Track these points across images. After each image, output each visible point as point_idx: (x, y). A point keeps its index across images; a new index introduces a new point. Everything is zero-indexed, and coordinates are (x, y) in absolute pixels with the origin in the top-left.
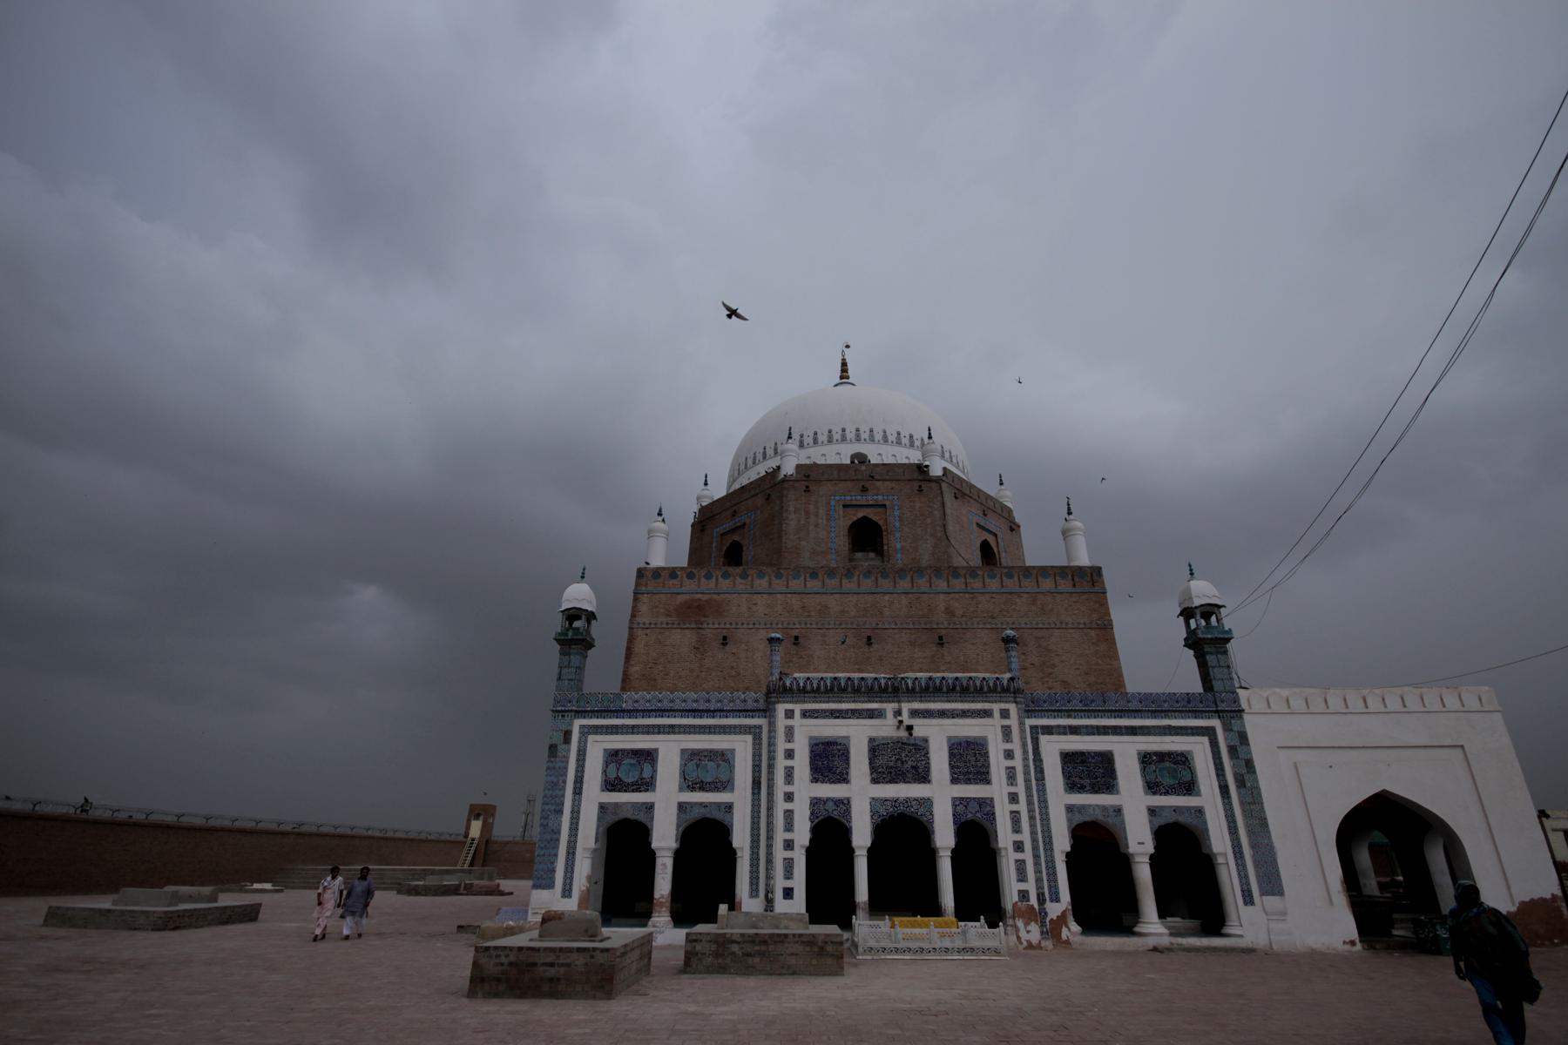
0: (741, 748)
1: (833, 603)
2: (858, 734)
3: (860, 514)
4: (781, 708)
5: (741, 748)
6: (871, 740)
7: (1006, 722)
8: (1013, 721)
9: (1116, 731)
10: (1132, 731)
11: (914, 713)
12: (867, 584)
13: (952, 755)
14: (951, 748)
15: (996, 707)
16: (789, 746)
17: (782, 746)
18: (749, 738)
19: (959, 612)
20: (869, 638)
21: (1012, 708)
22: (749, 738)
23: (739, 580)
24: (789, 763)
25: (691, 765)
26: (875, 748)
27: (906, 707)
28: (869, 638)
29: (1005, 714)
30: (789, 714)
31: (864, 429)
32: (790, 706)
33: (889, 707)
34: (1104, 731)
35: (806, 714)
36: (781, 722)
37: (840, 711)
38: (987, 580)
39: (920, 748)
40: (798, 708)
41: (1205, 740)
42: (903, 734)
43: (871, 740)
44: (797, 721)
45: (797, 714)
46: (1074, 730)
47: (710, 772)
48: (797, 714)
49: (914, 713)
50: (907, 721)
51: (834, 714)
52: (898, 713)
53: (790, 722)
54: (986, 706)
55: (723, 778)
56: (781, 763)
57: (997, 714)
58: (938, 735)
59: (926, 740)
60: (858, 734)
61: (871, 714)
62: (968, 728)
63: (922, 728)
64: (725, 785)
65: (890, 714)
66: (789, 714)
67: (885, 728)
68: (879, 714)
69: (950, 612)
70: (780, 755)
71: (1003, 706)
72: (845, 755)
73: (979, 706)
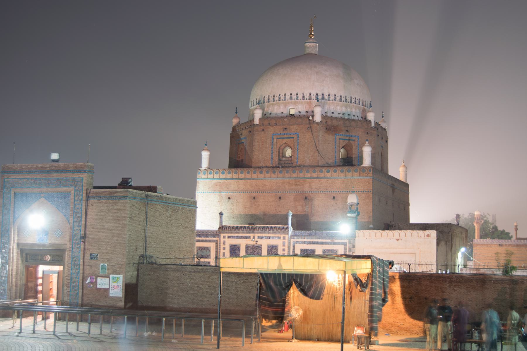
0: (212, 246)
1: (268, 183)
2: (243, 243)
3: (284, 142)
4: (222, 235)
5: (212, 246)
6: (246, 245)
7: (284, 240)
8: (286, 241)
9: (318, 243)
10: (322, 243)
11: (259, 237)
12: (281, 175)
13: (268, 250)
14: (268, 248)
15: (282, 236)
16: (224, 246)
17: (222, 246)
18: (215, 243)
19: (314, 187)
20: (280, 198)
21: (287, 236)
22: (215, 243)
23: (234, 175)
24: (224, 251)
25: (199, 251)
26: (247, 247)
27: (256, 235)
28: (280, 198)
29: (284, 238)
30: (224, 237)
31: (294, 93)
32: (224, 235)
33: (251, 235)
34: (314, 243)
35: (229, 237)
36: (222, 240)
37: (238, 236)
38: (326, 173)
39: (260, 247)
40: (227, 235)
41: (343, 247)
42: (255, 243)
43: (246, 245)
44: (226, 239)
45: (226, 237)
46: (304, 243)
47: (205, 253)
48: (226, 237)
49: (259, 237)
50: (256, 240)
51: (237, 237)
52: (254, 238)
53: (224, 239)
54: (279, 235)
55: (208, 255)
56: (222, 251)
57: (282, 238)
58: (264, 243)
59: (261, 245)
60: (243, 243)
61: (246, 237)
62: (273, 242)
63: (260, 242)
64: (208, 257)
65: (252, 237)
66: (224, 237)
67: (251, 242)
68: (249, 237)
69: (310, 187)
70: (222, 249)
71: (284, 235)
72: (239, 249)
73: (277, 235)
